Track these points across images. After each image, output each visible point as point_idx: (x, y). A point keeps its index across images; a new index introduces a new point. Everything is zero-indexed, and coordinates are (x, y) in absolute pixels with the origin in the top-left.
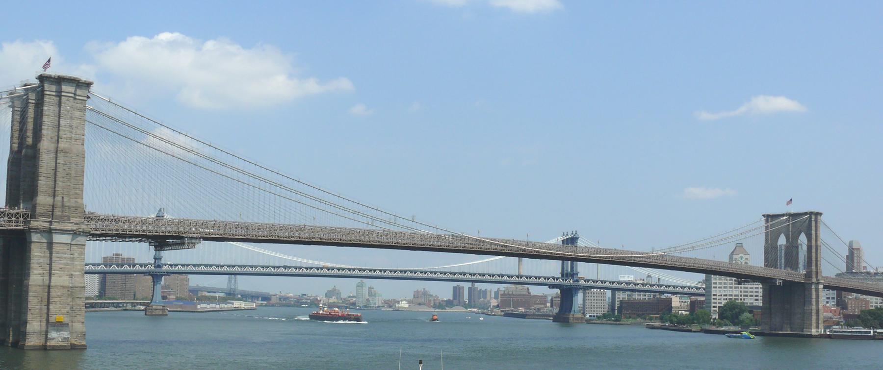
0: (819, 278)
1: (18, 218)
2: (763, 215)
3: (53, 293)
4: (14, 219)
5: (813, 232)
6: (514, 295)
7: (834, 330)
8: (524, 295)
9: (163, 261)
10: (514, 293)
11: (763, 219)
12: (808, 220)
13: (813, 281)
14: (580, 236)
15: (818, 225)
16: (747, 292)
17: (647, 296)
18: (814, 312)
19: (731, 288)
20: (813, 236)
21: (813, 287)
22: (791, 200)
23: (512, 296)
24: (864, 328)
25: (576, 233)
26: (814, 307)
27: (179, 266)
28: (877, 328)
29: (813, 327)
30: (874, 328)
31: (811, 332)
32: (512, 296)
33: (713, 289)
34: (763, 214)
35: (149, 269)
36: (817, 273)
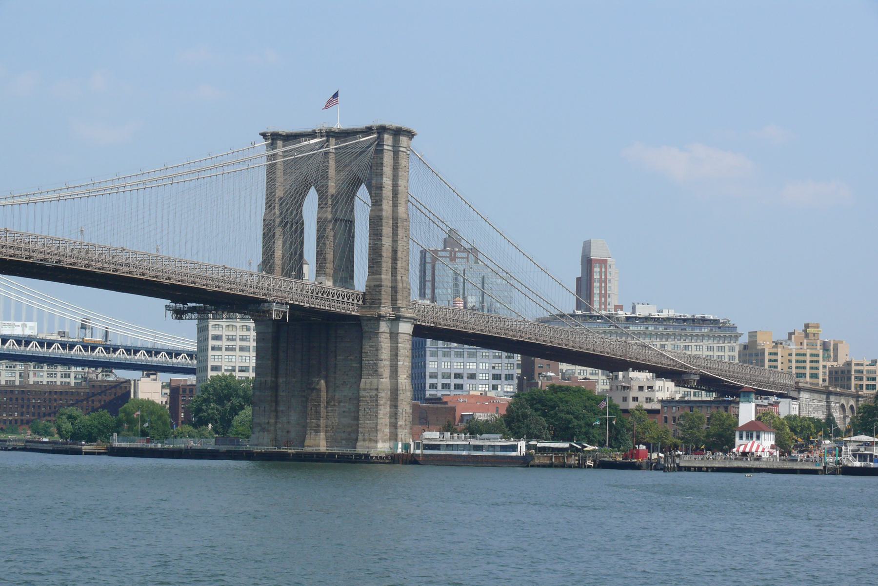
0: (400, 303)
5: (387, 182)
7: (424, 442)
11: (262, 143)
12: (373, 148)
13: (382, 313)
15: (403, 162)
17: (73, 375)
18: (384, 396)
20: (387, 192)
21: (384, 327)
22: (336, 95)
24: (505, 437)
26: (385, 381)
28: (538, 438)
29: (380, 435)
30: (530, 437)
31: (376, 448)
33: (211, 353)
34: (262, 131)
36: (394, 289)
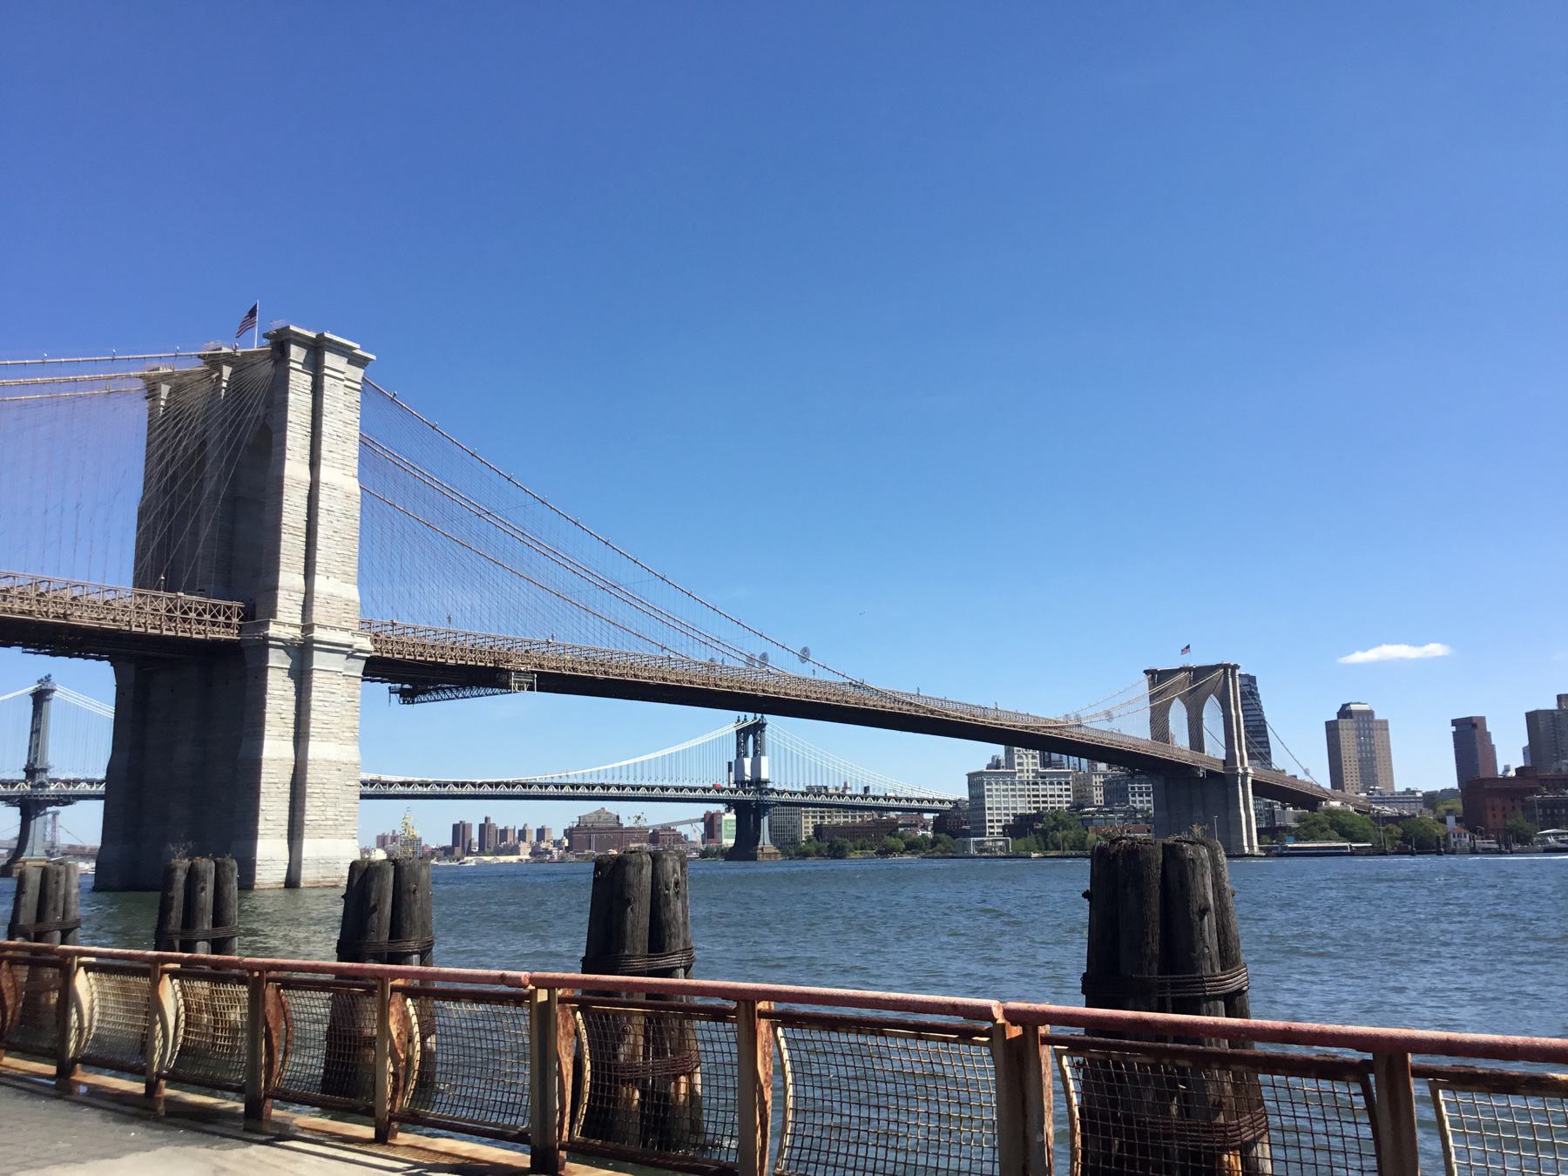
1: (228, 618)
2: (1146, 672)
3: (313, 775)
4: (221, 619)
6: (594, 829)
8: (612, 828)
9: (51, 775)
10: (596, 825)
12: (1222, 679)
14: (768, 721)
16: (1038, 802)
19: (1014, 796)
22: (1188, 647)
23: (593, 831)
27: (83, 784)
32: (593, 831)
33: (987, 799)
35: (22, 789)
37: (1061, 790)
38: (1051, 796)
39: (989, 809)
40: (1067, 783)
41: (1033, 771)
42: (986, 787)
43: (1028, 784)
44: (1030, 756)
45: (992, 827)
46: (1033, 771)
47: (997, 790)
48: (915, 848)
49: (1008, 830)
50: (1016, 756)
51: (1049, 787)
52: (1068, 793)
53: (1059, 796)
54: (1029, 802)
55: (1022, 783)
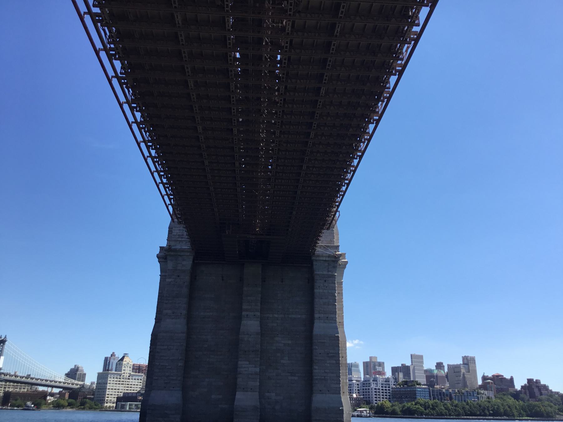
16: (128, 387)
25: (5, 337)
37: (138, 382)
38: (134, 385)
39: (108, 389)
40: (141, 380)
41: (129, 374)
42: (109, 379)
43: (126, 379)
44: (129, 367)
45: (108, 397)
46: (129, 374)
47: (113, 381)
48: (72, 405)
49: (119, 399)
50: (123, 366)
51: (134, 381)
52: (140, 384)
53: (137, 385)
54: (125, 387)
55: (123, 378)
